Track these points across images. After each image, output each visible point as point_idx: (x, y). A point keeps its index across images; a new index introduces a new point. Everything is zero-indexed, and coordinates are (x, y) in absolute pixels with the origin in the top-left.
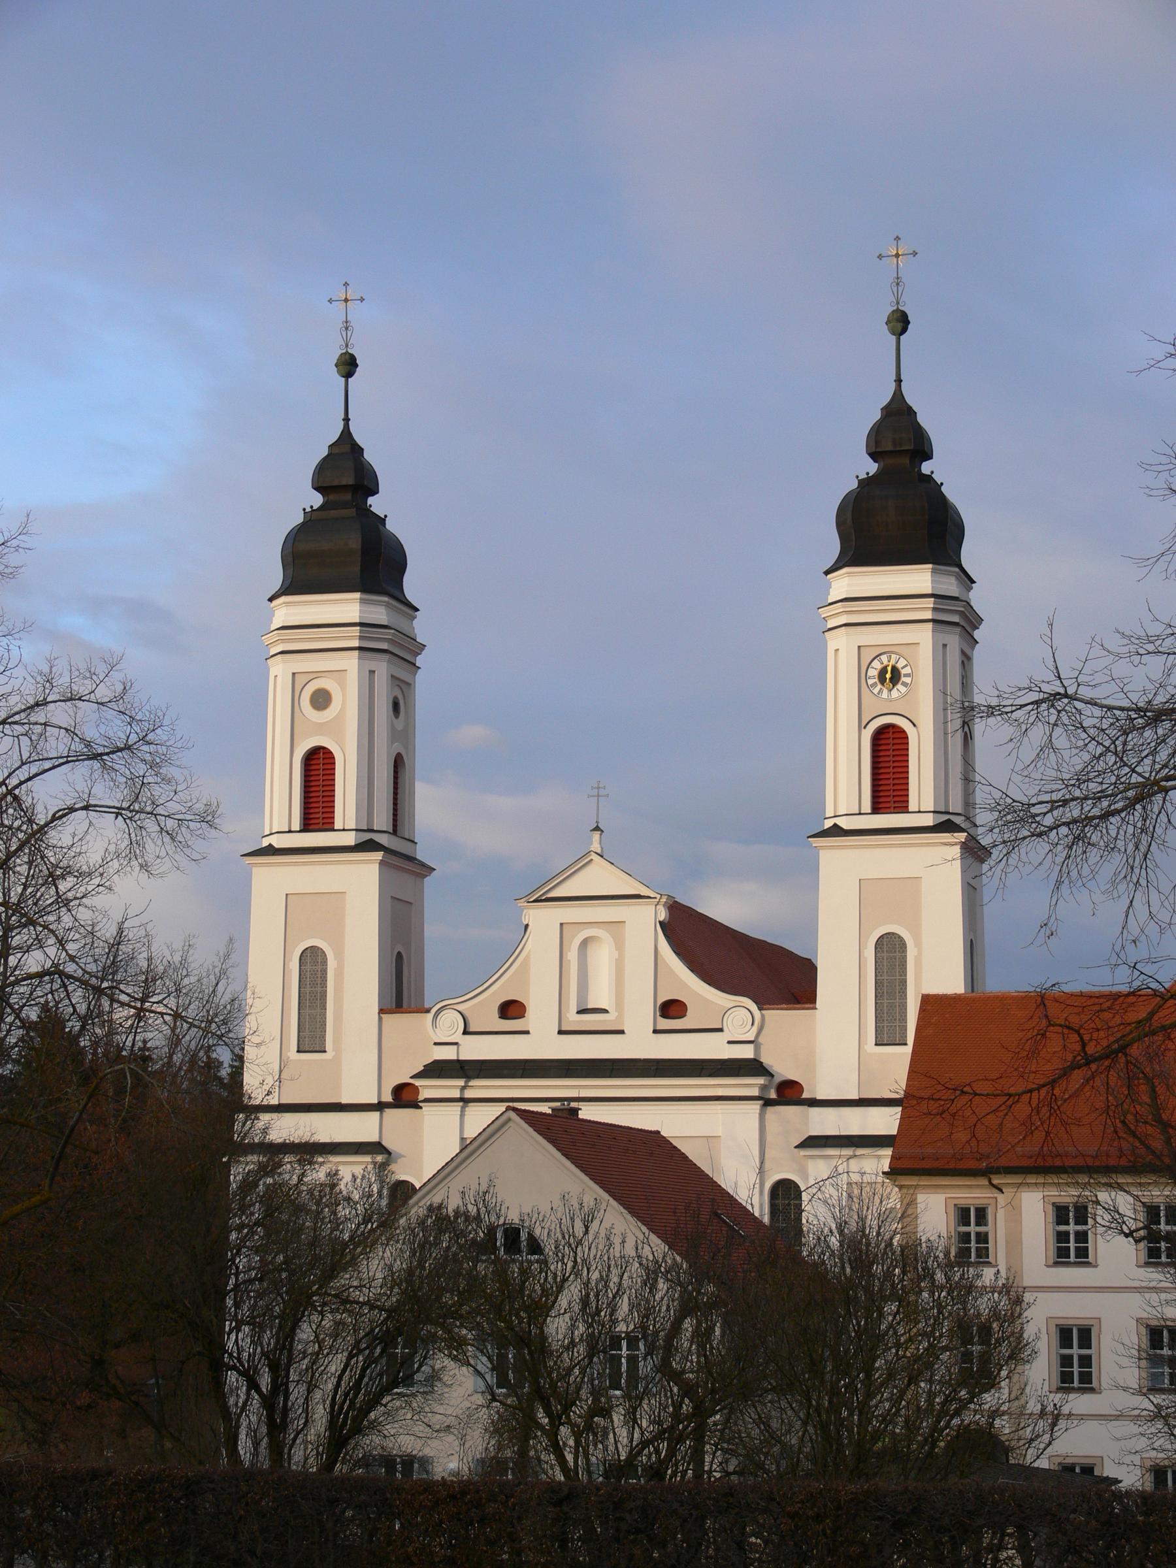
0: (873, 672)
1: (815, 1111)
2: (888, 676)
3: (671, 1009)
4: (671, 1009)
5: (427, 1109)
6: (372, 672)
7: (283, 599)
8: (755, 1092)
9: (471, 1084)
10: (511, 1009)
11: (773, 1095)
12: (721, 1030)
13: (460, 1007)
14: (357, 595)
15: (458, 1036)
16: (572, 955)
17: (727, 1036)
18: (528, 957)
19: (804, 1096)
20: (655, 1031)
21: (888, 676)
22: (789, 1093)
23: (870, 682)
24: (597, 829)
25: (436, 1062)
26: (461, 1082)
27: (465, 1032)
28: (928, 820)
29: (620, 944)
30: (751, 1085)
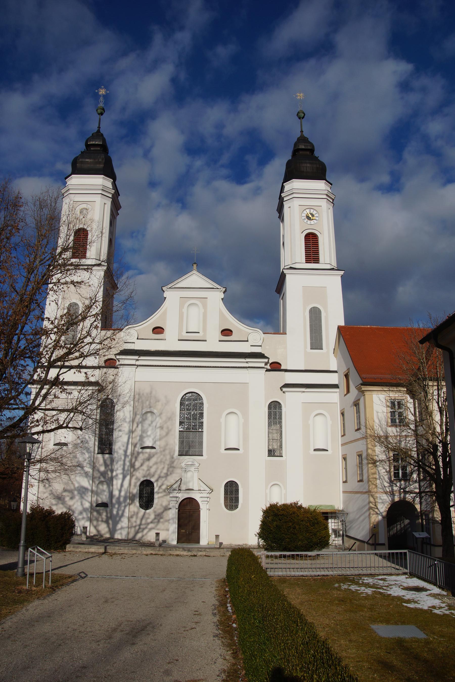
0: (304, 215)
1: (287, 373)
2: (310, 216)
3: (226, 332)
4: (226, 332)
5: (121, 369)
6: (105, 204)
7: (73, 176)
8: (263, 365)
9: (139, 358)
10: (158, 330)
11: (268, 367)
12: (248, 341)
13: (136, 328)
14: (102, 176)
15: (135, 340)
16: (185, 310)
17: (251, 342)
18: (166, 310)
19: (282, 368)
20: (220, 341)
21: (310, 216)
22: (276, 367)
23: (303, 218)
24: (195, 263)
25: (125, 350)
26: (136, 357)
27: (137, 339)
28: (329, 267)
29: (205, 306)
30: (260, 363)
